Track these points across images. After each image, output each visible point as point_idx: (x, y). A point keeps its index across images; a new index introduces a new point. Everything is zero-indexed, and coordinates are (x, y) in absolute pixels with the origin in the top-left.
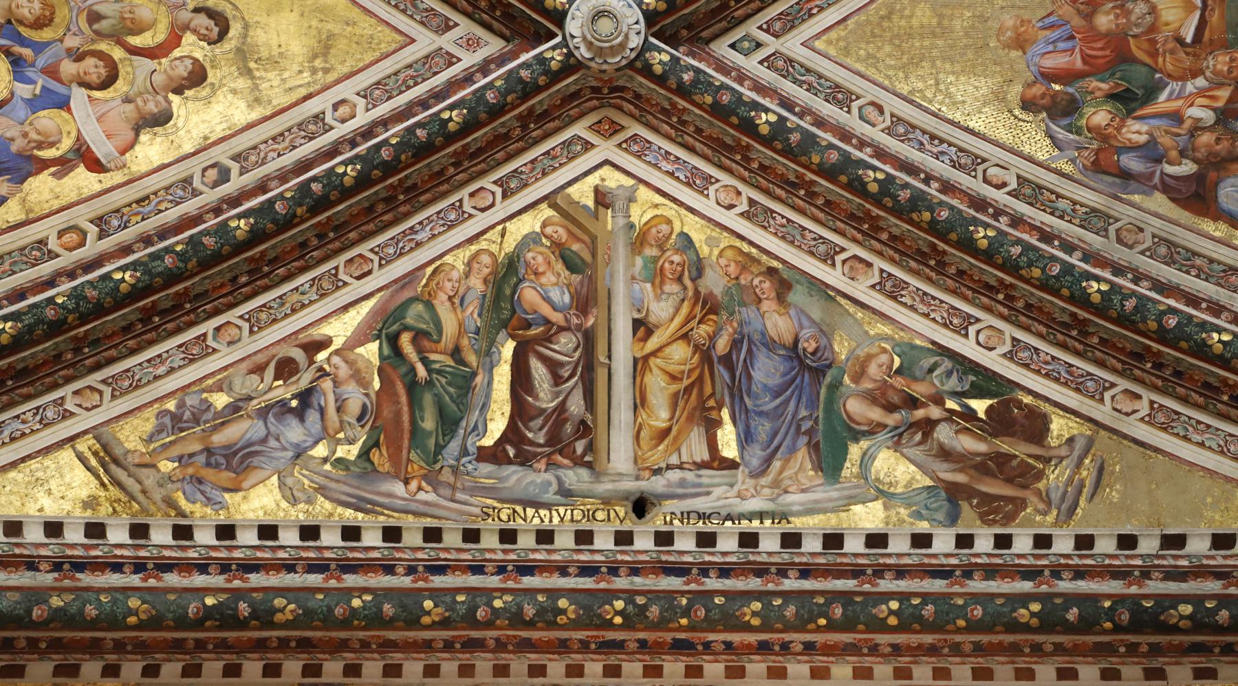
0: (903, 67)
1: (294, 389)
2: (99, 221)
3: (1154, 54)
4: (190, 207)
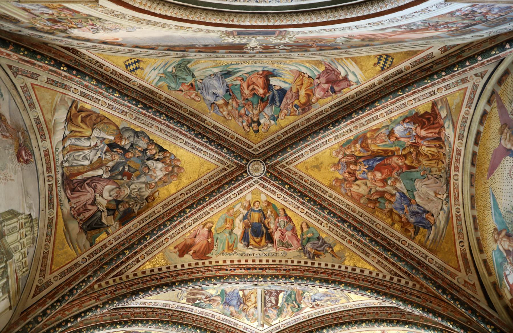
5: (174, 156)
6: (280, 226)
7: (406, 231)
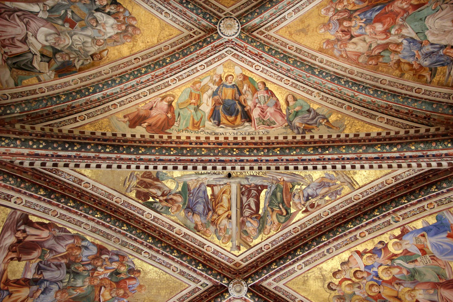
0: (168, 280)
1: (310, 201)
2: (356, 239)
3: (111, 284)
4: (336, 243)
5: (129, 13)
6: (260, 102)
7: (419, 77)
